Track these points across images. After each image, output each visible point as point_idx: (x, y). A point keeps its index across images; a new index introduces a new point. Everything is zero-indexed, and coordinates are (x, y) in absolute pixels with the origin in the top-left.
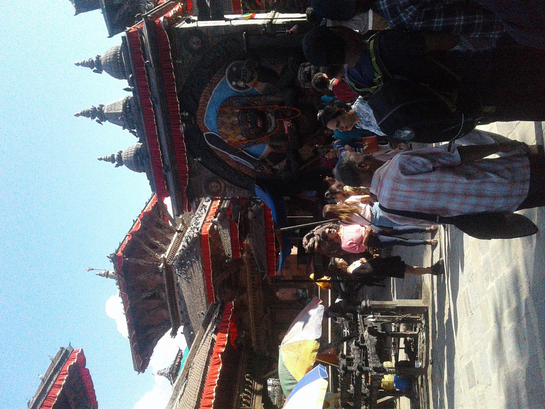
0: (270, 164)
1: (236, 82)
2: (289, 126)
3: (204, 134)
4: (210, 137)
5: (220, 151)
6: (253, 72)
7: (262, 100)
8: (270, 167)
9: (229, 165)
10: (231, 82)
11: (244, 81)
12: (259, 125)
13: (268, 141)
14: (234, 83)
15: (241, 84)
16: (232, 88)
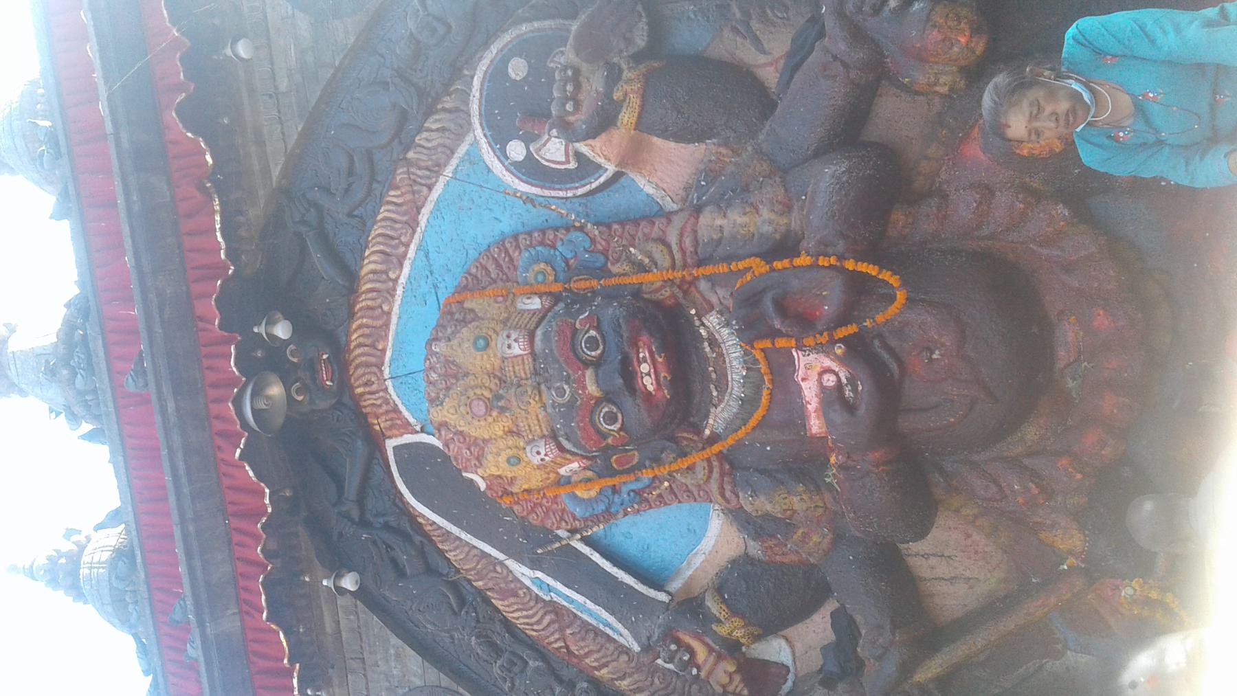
0: (732, 628)
1: (528, 139)
2: (830, 381)
3: (390, 444)
4: (413, 457)
5: (465, 544)
6: (614, 75)
7: (673, 239)
8: (732, 648)
9: (508, 625)
10: (499, 142)
11: (567, 131)
12: (649, 383)
13: (714, 486)
14: (516, 150)
15: (554, 150)
16: (509, 179)
